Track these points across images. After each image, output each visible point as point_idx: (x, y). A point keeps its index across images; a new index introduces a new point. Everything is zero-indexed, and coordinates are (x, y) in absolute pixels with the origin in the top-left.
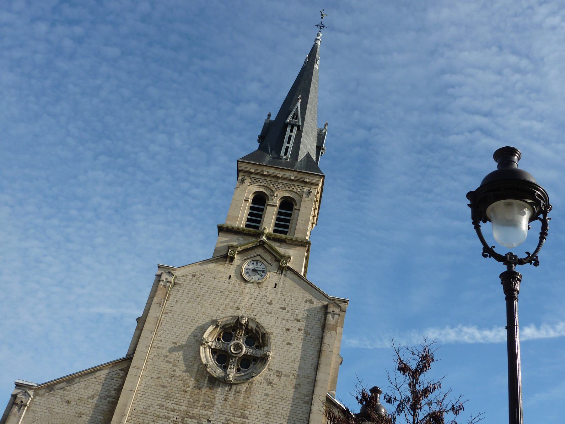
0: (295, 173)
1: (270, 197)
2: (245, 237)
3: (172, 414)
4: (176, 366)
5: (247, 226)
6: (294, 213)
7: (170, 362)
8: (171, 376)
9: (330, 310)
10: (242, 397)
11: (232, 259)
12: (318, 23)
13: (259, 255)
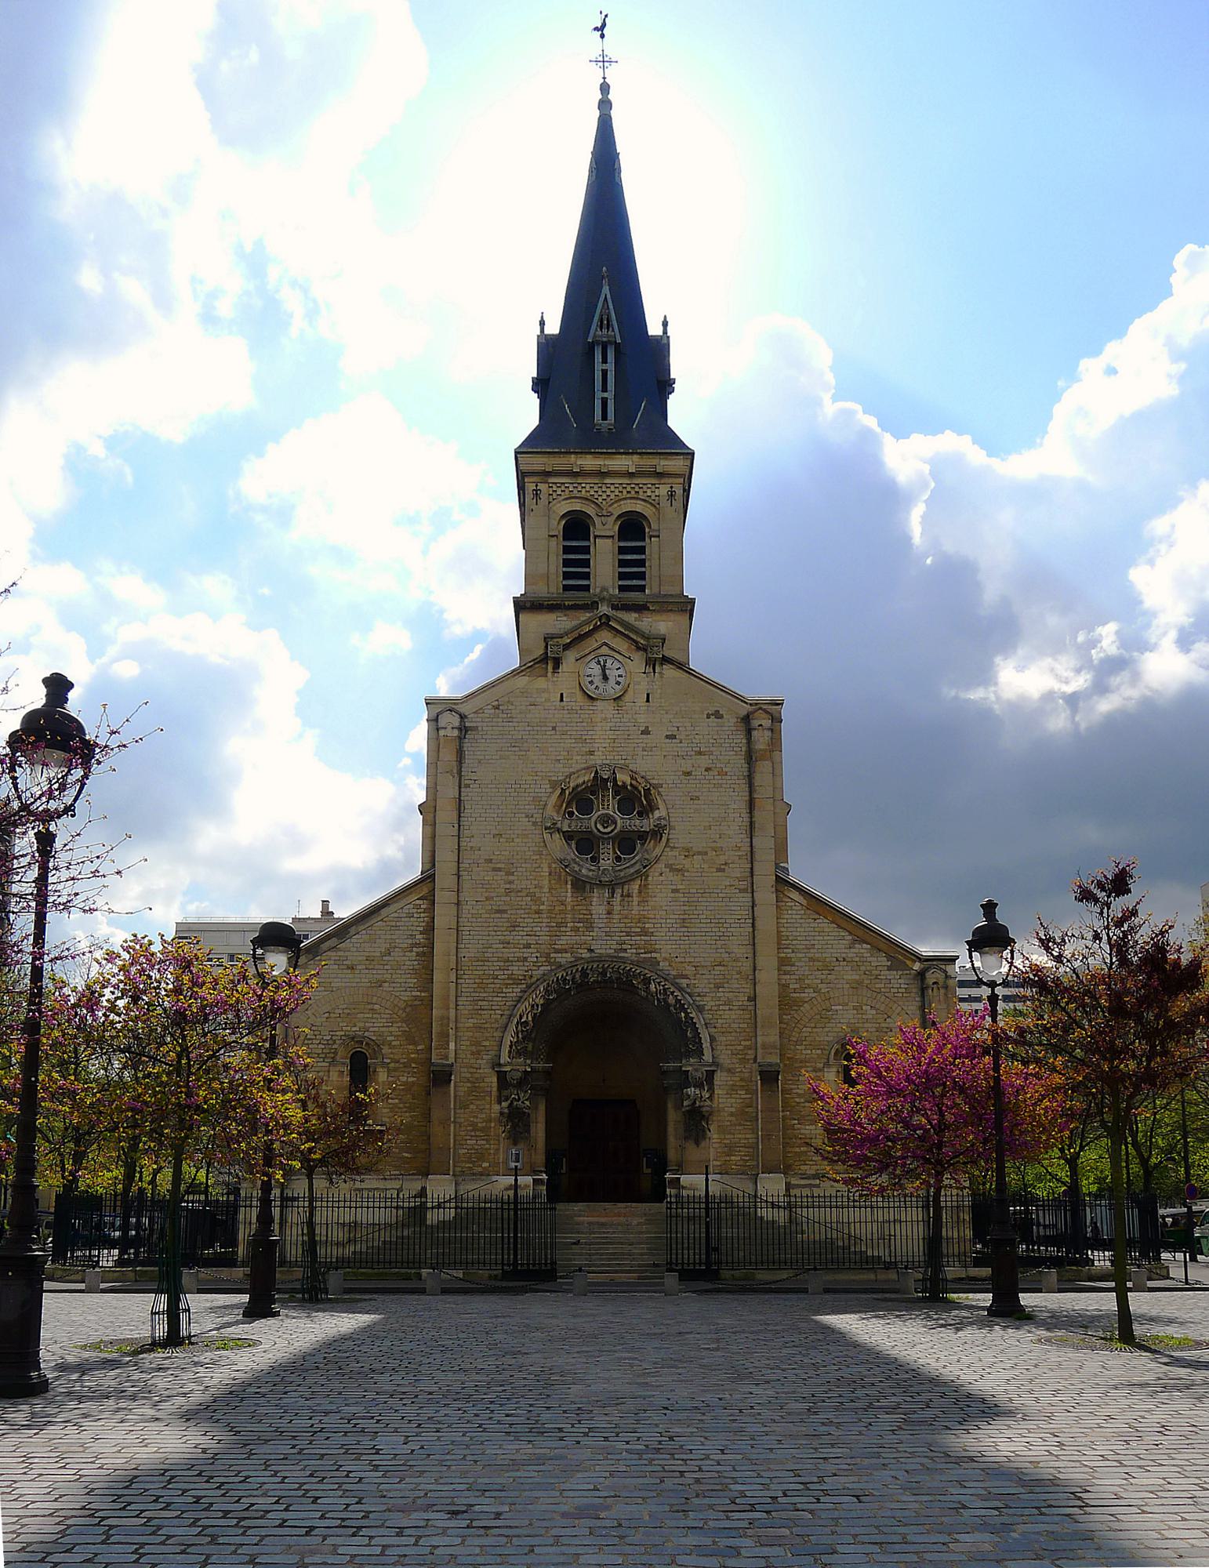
0: (635, 457)
1: (596, 519)
2: (571, 613)
3: (526, 952)
4: (512, 874)
5: (566, 588)
6: (652, 545)
7: (500, 869)
8: (508, 892)
9: (755, 723)
10: (635, 903)
11: (557, 663)
12: (596, 54)
13: (606, 644)
